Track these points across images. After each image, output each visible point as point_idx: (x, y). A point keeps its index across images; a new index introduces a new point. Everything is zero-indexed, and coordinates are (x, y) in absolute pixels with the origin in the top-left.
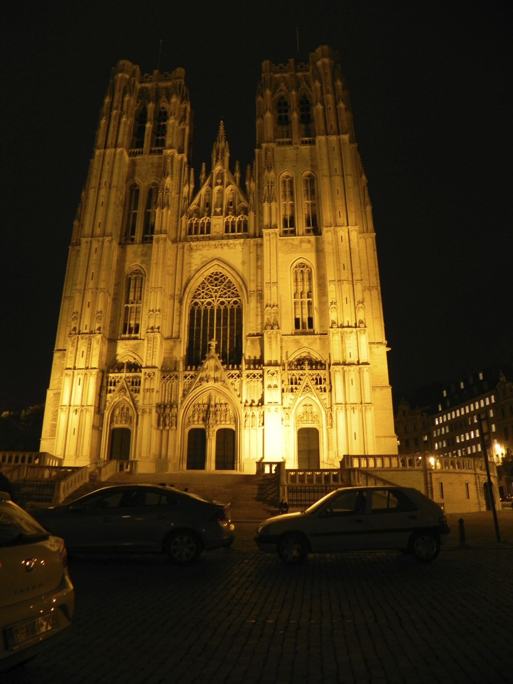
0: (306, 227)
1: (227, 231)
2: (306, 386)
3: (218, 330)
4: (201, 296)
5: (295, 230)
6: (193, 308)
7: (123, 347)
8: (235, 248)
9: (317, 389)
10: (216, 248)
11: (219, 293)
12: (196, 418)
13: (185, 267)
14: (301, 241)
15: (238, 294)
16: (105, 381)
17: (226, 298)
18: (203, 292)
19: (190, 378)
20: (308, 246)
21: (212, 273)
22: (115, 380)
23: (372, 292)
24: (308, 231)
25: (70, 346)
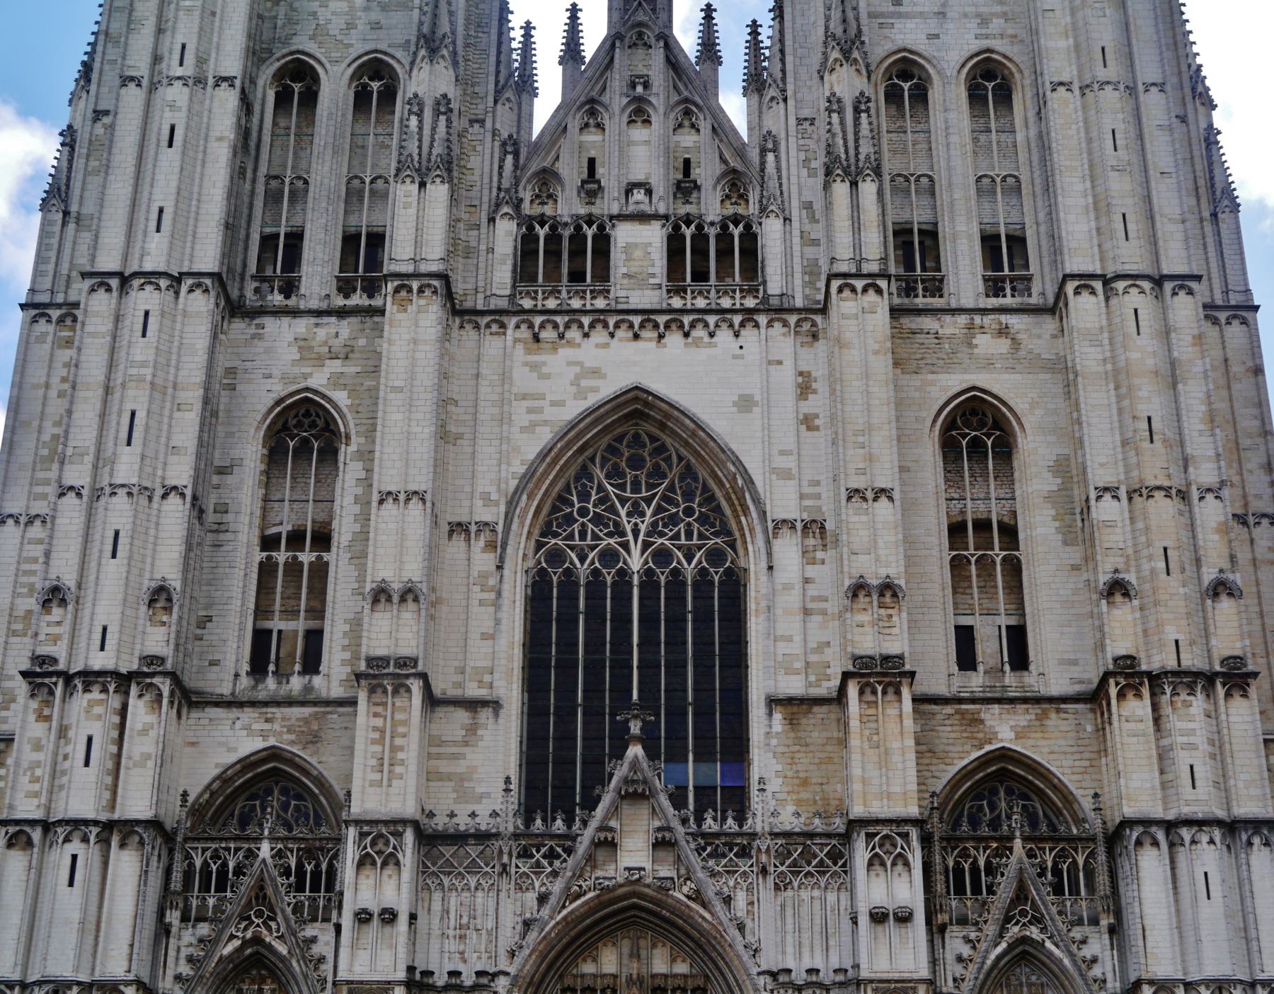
0: (985, 268)
2: (1018, 897)
3: (648, 667)
5: (941, 280)
6: (542, 573)
7: (256, 726)
8: (710, 345)
9: (1060, 913)
11: (648, 519)
14: (970, 327)
15: (724, 524)
17: (676, 537)
18: (583, 512)
19: (545, 862)
20: (1003, 345)
21: (620, 439)
22: (225, 865)
23: (1257, 532)
24: (995, 287)
25: (32, 718)
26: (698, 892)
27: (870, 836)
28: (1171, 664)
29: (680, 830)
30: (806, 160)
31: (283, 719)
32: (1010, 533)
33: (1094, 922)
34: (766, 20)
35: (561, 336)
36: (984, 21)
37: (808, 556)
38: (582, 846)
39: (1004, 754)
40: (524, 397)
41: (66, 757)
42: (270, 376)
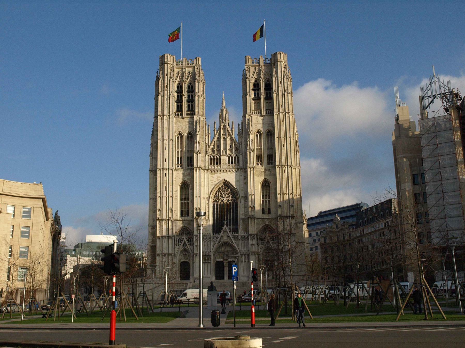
1: (229, 163)
4: (218, 197)
5: (262, 163)
10: (224, 172)
11: (226, 196)
12: (219, 257)
13: (209, 182)
16: (176, 240)
17: (230, 198)
18: (219, 195)
22: (180, 240)
26: (232, 242)
27: (251, 236)
28: (285, 215)
29: (230, 235)
30: (245, 147)
31: (185, 222)
32: (269, 196)
33: (276, 244)
34: (240, 123)
35: (215, 172)
36: (269, 124)
37: (245, 201)
38: (220, 237)
39: (267, 225)
40: (211, 181)
41: (163, 229)
42: (180, 179)
